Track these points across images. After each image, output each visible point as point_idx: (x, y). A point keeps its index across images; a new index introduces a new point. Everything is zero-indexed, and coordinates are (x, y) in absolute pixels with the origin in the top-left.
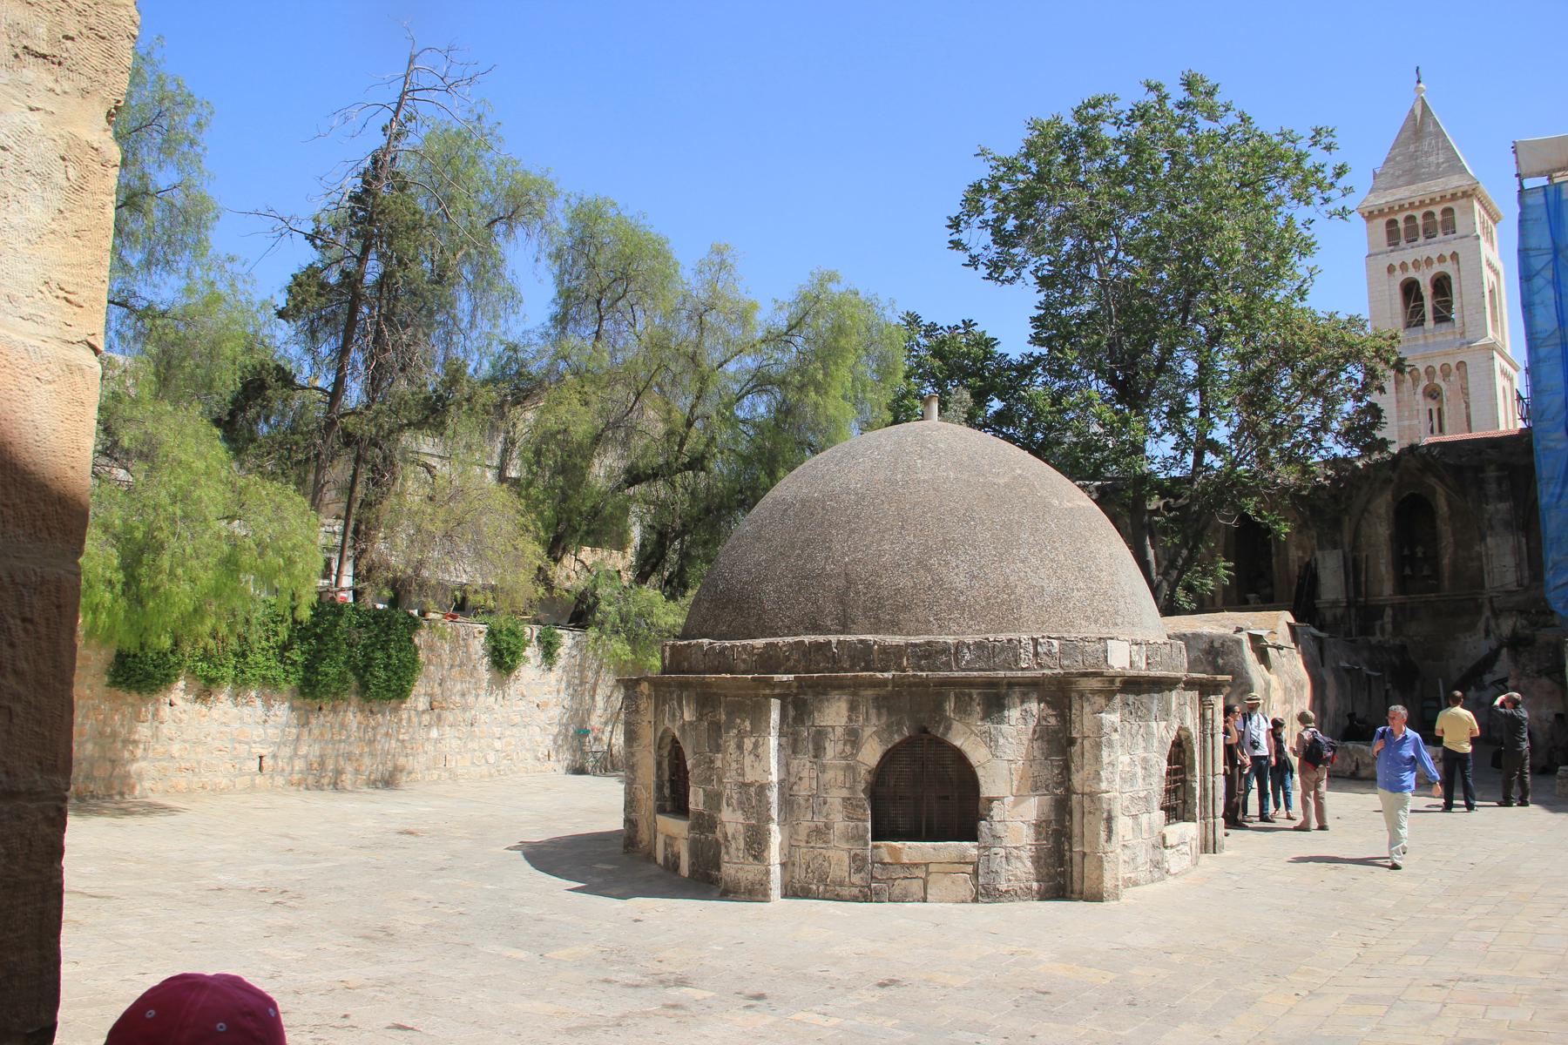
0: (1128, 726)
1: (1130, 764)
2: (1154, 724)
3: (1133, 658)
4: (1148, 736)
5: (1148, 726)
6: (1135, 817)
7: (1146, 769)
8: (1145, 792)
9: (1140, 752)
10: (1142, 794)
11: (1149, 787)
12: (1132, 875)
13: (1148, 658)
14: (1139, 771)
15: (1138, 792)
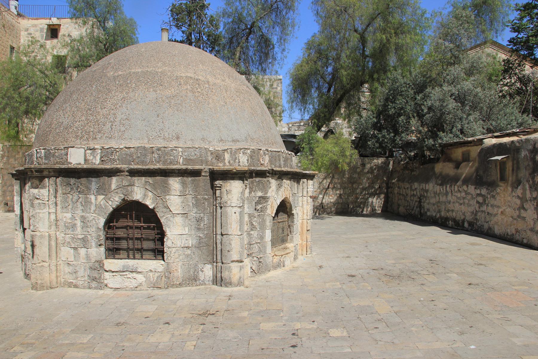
0: (71, 197)
1: (71, 219)
2: (93, 197)
3: (88, 158)
4: (87, 203)
5: (87, 198)
6: (75, 249)
7: (83, 222)
8: (83, 236)
9: (79, 213)
10: (80, 237)
11: (87, 233)
12: (74, 281)
13: (102, 157)
14: (79, 223)
15: (77, 234)
